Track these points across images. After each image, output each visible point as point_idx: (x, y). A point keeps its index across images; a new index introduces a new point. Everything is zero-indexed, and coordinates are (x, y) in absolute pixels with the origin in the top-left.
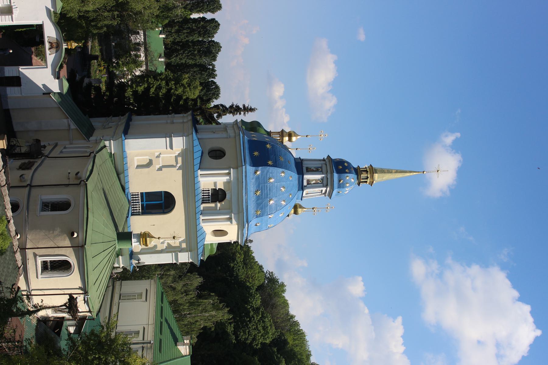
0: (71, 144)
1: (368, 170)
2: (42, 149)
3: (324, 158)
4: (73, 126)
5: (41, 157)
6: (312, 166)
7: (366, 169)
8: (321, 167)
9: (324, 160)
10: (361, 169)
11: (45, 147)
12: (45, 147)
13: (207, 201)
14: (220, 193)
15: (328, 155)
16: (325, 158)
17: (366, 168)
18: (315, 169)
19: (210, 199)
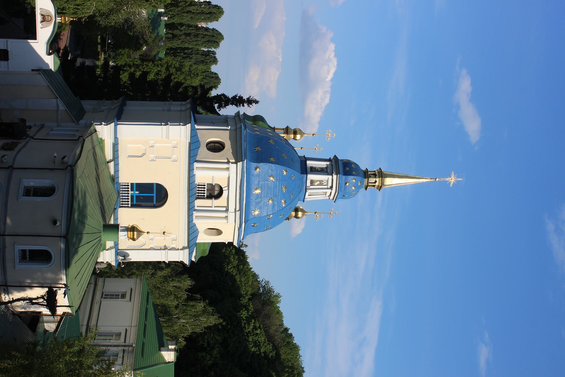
1: (377, 174)
2: (27, 130)
4: (62, 107)
5: (26, 138)
7: (374, 173)
10: (369, 173)
11: (30, 127)
12: (30, 127)
13: (202, 197)
16: (332, 158)
17: (375, 171)
18: (319, 169)
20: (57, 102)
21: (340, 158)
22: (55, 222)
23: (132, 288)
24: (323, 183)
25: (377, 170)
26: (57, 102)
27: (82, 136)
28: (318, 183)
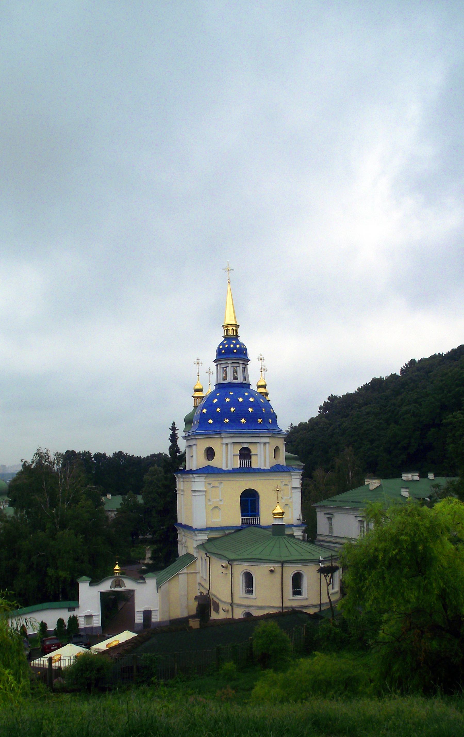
0: (199, 573)
1: (226, 329)
2: (203, 594)
3: (216, 365)
4: (185, 571)
6: (222, 375)
7: (226, 331)
8: (223, 368)
9: (217, 365)
10: (226, 335)
13: (250, 462)
14: (243, 452)
15: (214, 361)
16: (215, 364)
18: (225, 373)
19: (248, 460)
20: (180, 574)
21: (215, 358)
22: (272, 571)
23: (324, 513)
24: (235, 370)
25: (224, 328)
26: (180, 574)
27: (206, 554)
28: (235, 374)
